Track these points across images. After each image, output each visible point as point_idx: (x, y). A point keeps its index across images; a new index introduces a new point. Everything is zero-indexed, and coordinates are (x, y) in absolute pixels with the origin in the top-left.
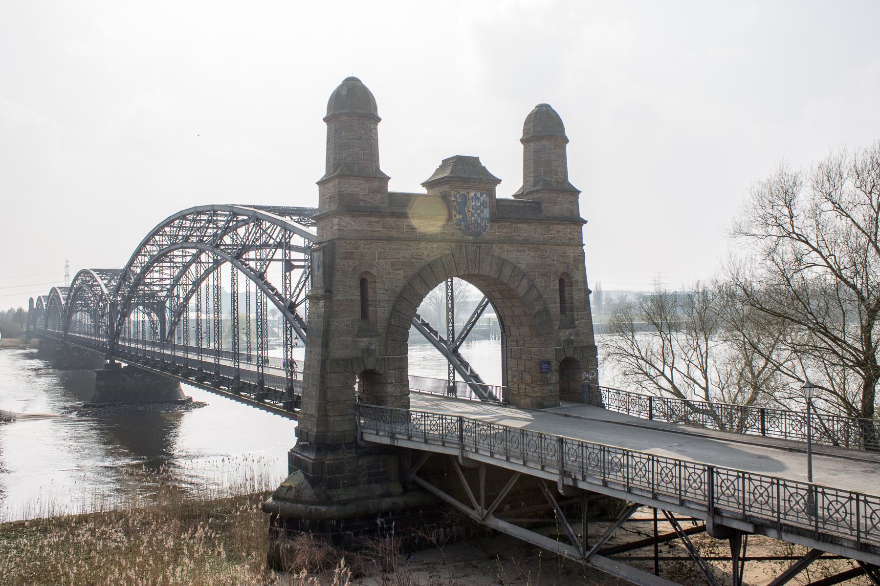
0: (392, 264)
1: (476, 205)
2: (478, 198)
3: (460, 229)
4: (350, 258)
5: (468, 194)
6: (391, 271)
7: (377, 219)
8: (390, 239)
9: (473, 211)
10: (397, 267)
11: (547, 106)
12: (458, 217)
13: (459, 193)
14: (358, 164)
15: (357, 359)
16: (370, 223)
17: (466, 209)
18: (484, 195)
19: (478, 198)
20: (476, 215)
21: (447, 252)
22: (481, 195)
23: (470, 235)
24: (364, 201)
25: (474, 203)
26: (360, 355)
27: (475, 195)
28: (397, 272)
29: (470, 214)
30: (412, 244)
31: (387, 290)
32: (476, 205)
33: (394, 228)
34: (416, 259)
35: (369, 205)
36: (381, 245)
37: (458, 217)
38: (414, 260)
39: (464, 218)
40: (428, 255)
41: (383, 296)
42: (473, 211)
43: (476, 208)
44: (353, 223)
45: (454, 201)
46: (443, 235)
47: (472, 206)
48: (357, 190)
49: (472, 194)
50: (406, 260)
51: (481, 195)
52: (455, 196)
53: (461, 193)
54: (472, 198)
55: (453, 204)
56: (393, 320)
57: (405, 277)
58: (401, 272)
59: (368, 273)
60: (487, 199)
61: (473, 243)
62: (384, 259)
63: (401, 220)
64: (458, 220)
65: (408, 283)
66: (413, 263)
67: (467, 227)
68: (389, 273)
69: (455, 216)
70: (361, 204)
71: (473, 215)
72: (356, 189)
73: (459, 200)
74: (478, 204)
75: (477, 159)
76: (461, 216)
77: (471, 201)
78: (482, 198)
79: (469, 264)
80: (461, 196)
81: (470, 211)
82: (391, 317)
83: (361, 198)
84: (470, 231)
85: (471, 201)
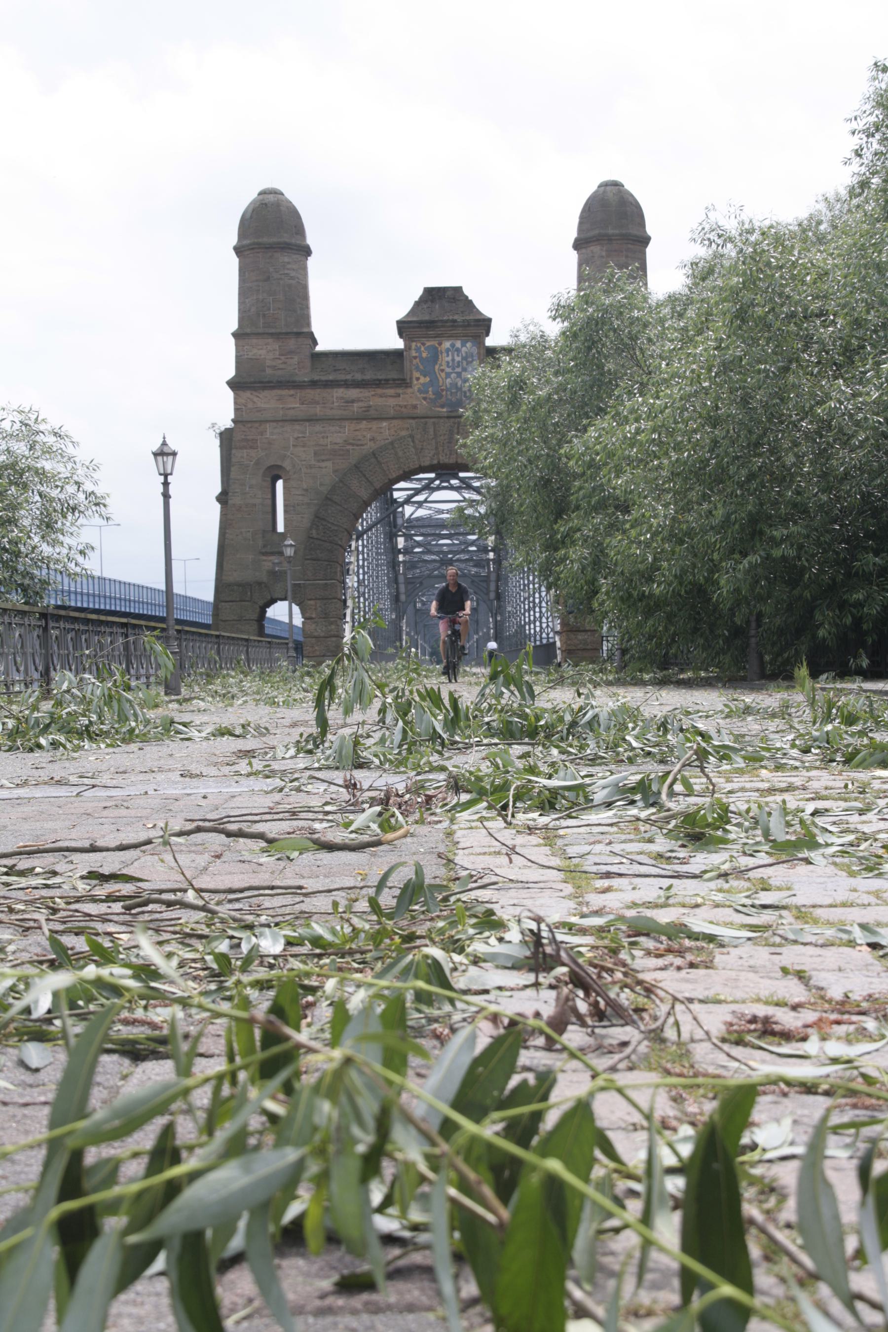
0: (315, 454)
1: (453, 360)
2: (458, 350)
3: (425, 399)
4: (251, 447)
5: (440, 344)
6: (313, 462)
7: (292, 392)
8: (312, 420)
9: (449, 370)
10: (323, 457)
11: (616, 184)
12: (423, 380)
13: (423, 344)
14: (264, 315)
15: (260, 584)
16: (280, 399)
17: (437, 367)
18: (469, 345)
19: (458, 350)
20: (453, 375)
21: (404, 433)
22: (463, 345)
23: (442, 406)
24: (274, 367)
25: (450, 358)
26: (265, 579)
27: (453, 345)
28: (323, 464)
29: (443, 375)
30: (347, 424)
31: (306, 490)
32: (453, 360)
33: (318, 403)
34: (353, 445)
35: (280, 372)
36: (297, 427)
37: (423, 380)
38: (350, 447)
39: (434, 381)
40: (373, 439)
41: (301, 498)
42: (449, 370)
43: (454, 365)
44: (255, 399)
45: (415, 358)
46: (398, 408)
47: (448, 362)
48: (263, 352)
49: (447, 344)
50: (337, 447)
51: (463, 345)
52: (418, 350)
53: (428, 344)
54: (448, 350)
55: (415, 362)
56: (314, 532)
57: (335, 471)
58: (329, 464)
59: (280, 467)
60: (475, 350)
61: (448, 417)
62: (303, 446)
63: (329, 390)
64: (423, 385)
65: (341, 481)
66: (348, 451)
67: (438, 394)
68: (311, 467)
69: (418, 379)
70: (269, 371)
71: (448, 375)
72: (260, 352)
73: (424, 355)
74: (458, 359)
75: (459, 290)
76: (428, 379)
77: (445, 355)
78: (464, 349)
79: (440, 449)
80: (428, 349)
81: (442, 371)
82: (311, 528)
83: (268, 363)
84: (443, 399)
85: (445, 355)
